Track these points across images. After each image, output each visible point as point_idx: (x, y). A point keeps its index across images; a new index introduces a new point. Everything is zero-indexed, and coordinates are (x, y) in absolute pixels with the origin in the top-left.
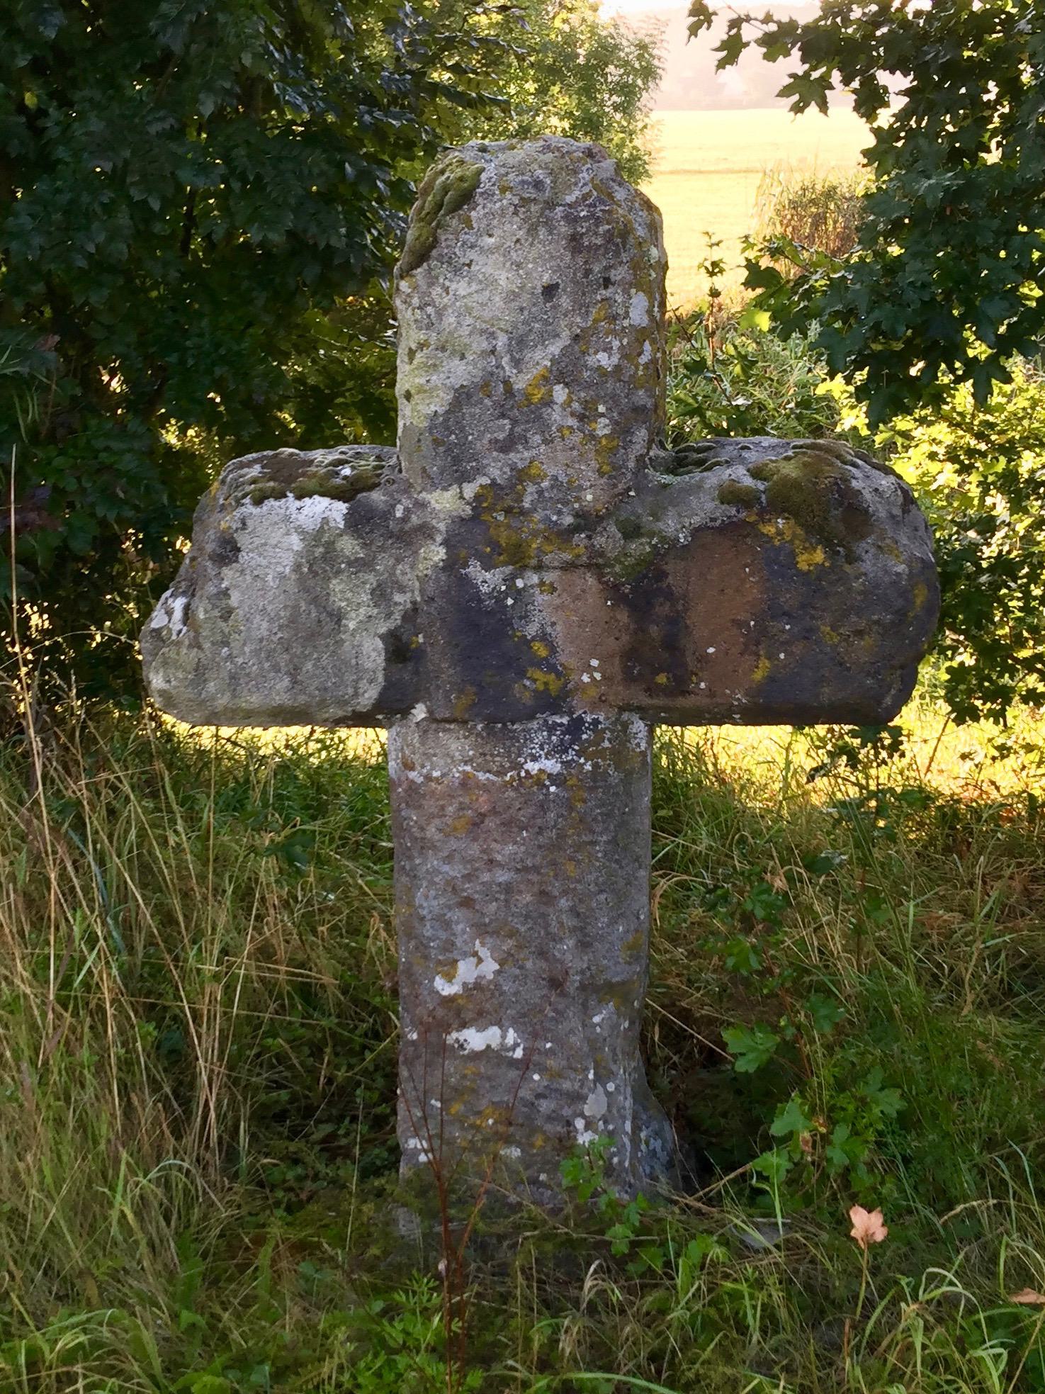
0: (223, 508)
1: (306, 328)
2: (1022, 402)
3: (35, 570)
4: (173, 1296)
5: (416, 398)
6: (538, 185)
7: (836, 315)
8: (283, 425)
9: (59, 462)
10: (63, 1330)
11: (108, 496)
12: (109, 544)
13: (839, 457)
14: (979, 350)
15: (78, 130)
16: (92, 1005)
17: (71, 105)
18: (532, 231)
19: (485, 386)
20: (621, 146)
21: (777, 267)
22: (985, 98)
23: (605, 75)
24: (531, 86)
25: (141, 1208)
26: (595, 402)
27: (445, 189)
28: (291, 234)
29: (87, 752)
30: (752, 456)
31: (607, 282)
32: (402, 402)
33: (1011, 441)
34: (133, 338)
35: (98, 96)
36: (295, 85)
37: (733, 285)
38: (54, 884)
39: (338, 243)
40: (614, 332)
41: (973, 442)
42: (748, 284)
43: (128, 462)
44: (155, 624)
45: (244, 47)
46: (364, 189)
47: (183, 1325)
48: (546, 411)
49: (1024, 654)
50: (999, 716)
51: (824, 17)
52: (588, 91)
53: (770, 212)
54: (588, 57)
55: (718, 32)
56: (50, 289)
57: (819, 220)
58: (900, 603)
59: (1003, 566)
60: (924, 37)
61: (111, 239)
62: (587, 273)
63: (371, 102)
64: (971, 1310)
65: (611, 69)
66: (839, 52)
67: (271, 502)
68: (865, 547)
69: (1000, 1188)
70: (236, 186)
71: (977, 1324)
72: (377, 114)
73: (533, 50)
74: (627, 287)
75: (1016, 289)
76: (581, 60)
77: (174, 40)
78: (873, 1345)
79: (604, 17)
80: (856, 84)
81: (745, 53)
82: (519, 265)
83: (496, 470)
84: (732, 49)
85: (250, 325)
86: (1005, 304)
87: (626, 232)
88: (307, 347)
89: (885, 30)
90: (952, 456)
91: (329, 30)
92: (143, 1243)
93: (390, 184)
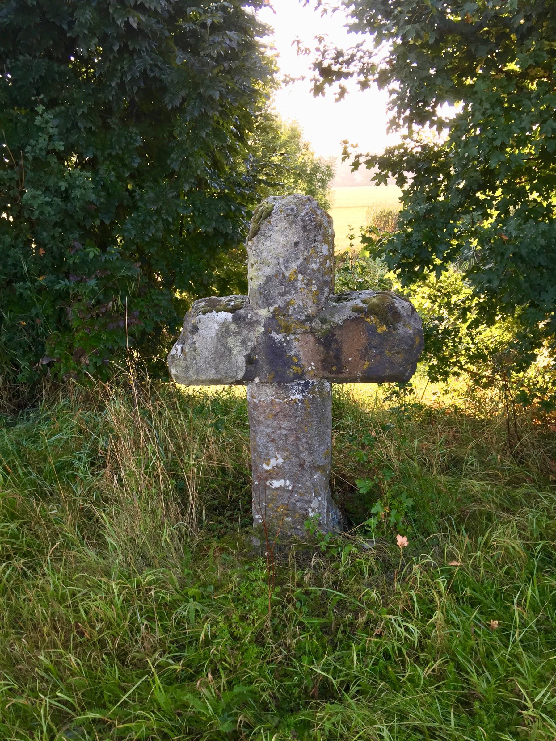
0: (193, 316)
1: (220, 259)
2: (452, 279)
3: (135, 338)
4: (182, 565)
5: (254, 280)
6: (292, 210)
7: (390, 251)
8: (213, 291)
9: (142, 303)
10: (147, 575)
11: (157, 313)
12: (158, 330)
13: (391, 296)
14: (438, 261)
15: (146, 196)
16: (155, 474)
17: (143, 188)
18: (291, 224)
19: (276, 275)
20: (321, 199)
21: (371, 236)
22: (439, 179)
23: (316, 176)
24: (292, 180)
25: (172, 536)
26: (312, 280)
27: (262, 212)
28: (214, 229)
29: (152, 395)
30: (363, 297)
31: (315, 241)
32: (249, 281)
33: (449, 292)
34: (164, 263)
35: (152, 185)
36: (215, 180)
37: (358, 245)
38: (142, 436)
39: (230, 232)
40: (317, 257)
41: (436, 293)
42: (362, 242)
43: (164, 303)
44: (172, 353)
45: (197, 168)
46: (237, 214)
47: (186, 573)
48: (296, 283)
49: (453, 360)
50: (445, 380)
51: (386, 154)
52: (311, 181)
53: (370, 220)
54: (310, 171)
55: (352, 160)
56: (138, 248)
57: (386, 222)
58: (411, 343)
59: (446, 332)
60: (418, 160)
61: (157, 231)
62: (308, 238)
63: (240, 185)
64: (435, 568)
65: (318, 174)
66: (391, 165)
67: (208, 314)
68: (399, 325)
69: (445, 529)
70: (196, 214)
71: (438, 572)
72: (242, 189)
73: (292, 168)
74: (321, 242)
75: (449, 241)
76: (308, 172)
77: (176, 167)
78: (404, 579)
79: (316, 157)
80: (396, 176)
81: (360, 167)
82: (286, 236)
83: (280, 302)
84: (356, 165)
85: (202, 259)
86: (445, 246)
87: (321, 225)
88: (220, 266)
89: (406, 158)
90: (429, 297)
91: (225, 162)
92: (173, 548)
93: (246, 212)
